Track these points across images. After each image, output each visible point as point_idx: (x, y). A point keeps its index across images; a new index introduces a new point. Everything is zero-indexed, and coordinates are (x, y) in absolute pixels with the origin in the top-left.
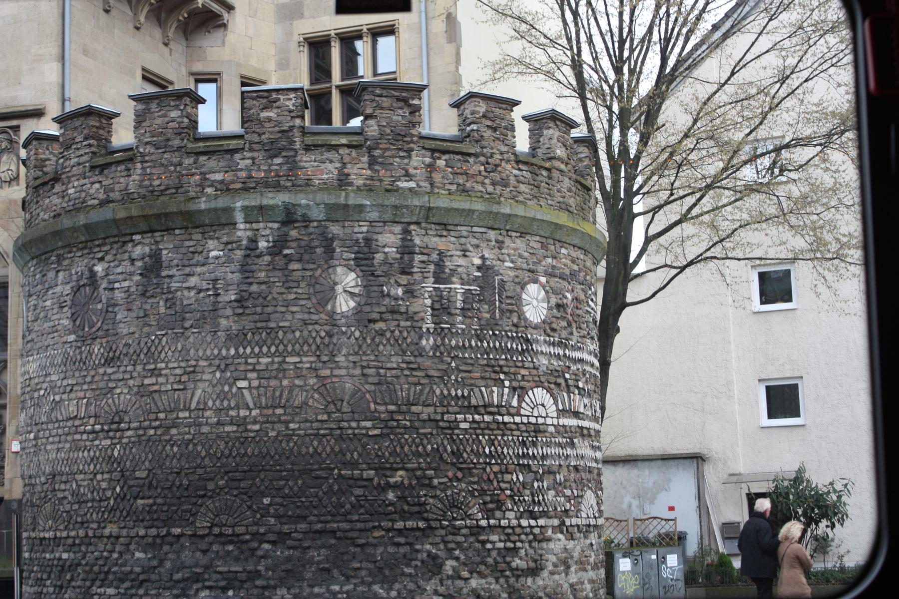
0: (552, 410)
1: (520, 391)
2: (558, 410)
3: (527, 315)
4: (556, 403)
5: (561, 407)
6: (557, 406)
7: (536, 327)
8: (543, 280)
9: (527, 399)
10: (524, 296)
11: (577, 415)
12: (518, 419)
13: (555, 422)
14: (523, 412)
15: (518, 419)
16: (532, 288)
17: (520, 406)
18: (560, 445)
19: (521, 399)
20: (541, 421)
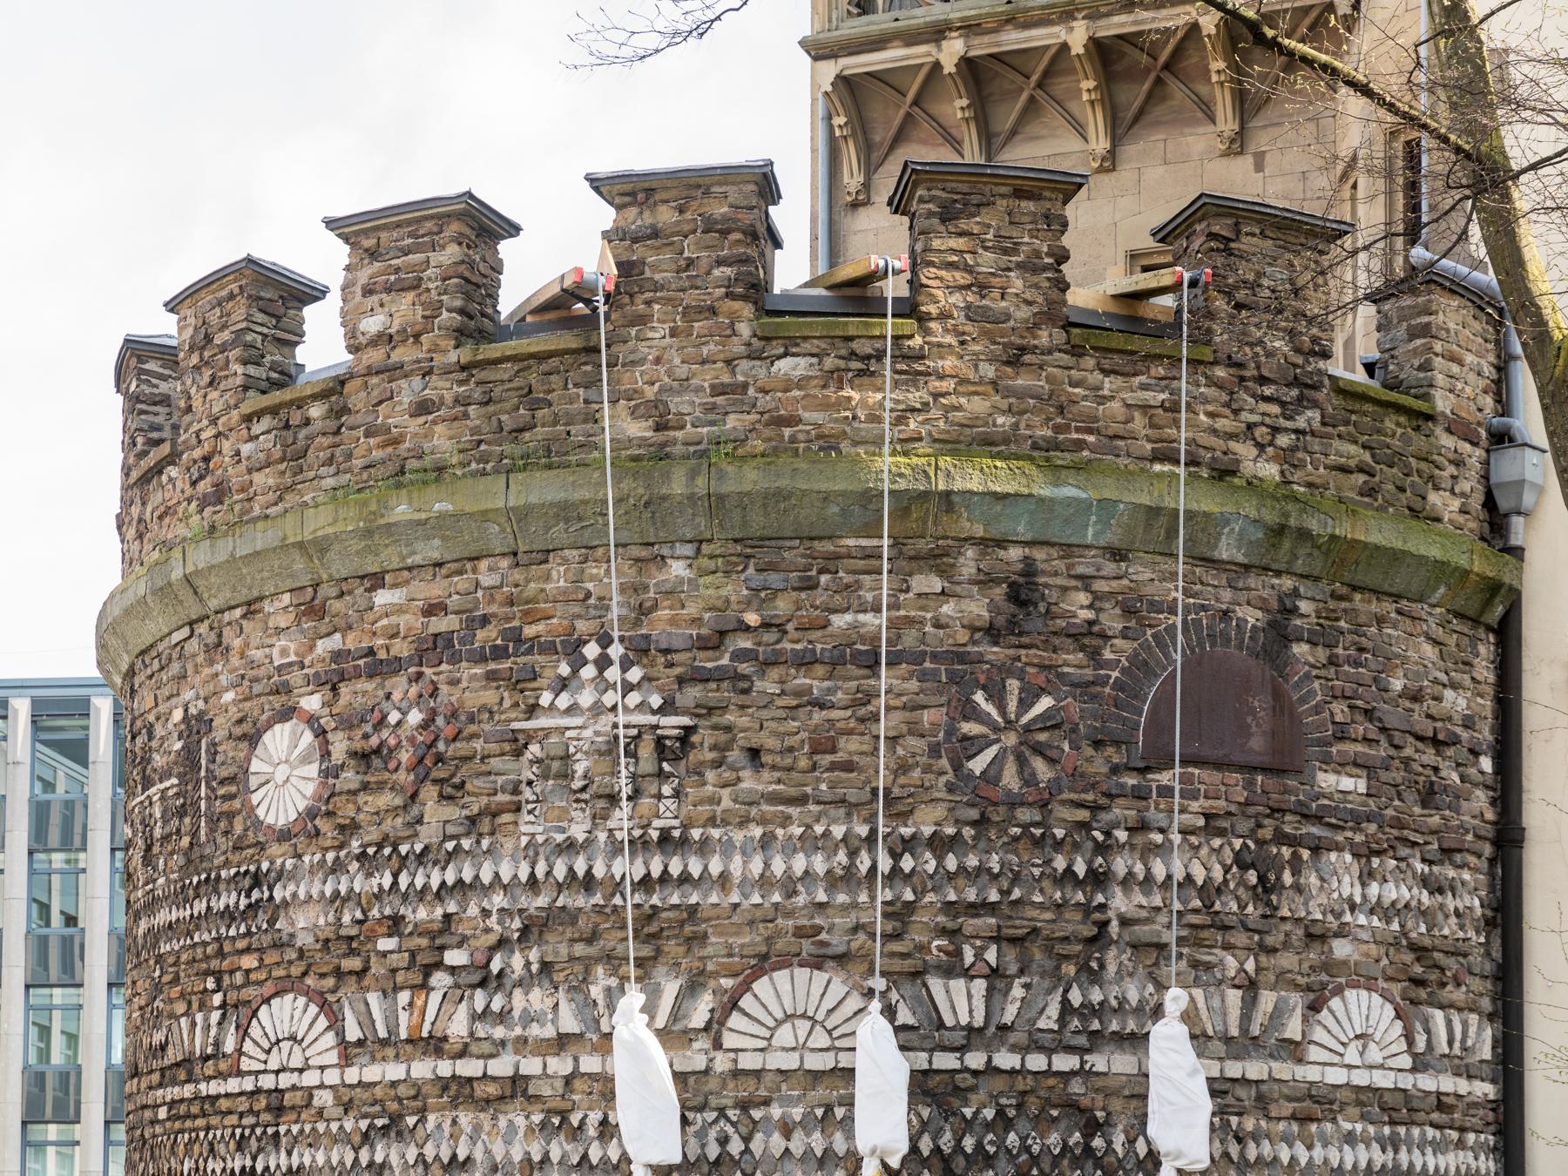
0: (324, 1048)
1: (242, 1012)
2: (342, 1043)
3: (261, 812)
4: (336, 1024)
5: (353, 1033)
6: (341, 1034)
7: (284, 835)
8: (312, 703)
9: (255, 1031)
10: (255, 766)
11: (435, 1045)
12: (233, 1085)
13: (332, 1077)
14: (246, 1064)
15: (233, 1085)
16: (280, 740)
17: (239, 1052)
18: (342, 1138)
19: (243, 1032)
20: (285, 1081)
